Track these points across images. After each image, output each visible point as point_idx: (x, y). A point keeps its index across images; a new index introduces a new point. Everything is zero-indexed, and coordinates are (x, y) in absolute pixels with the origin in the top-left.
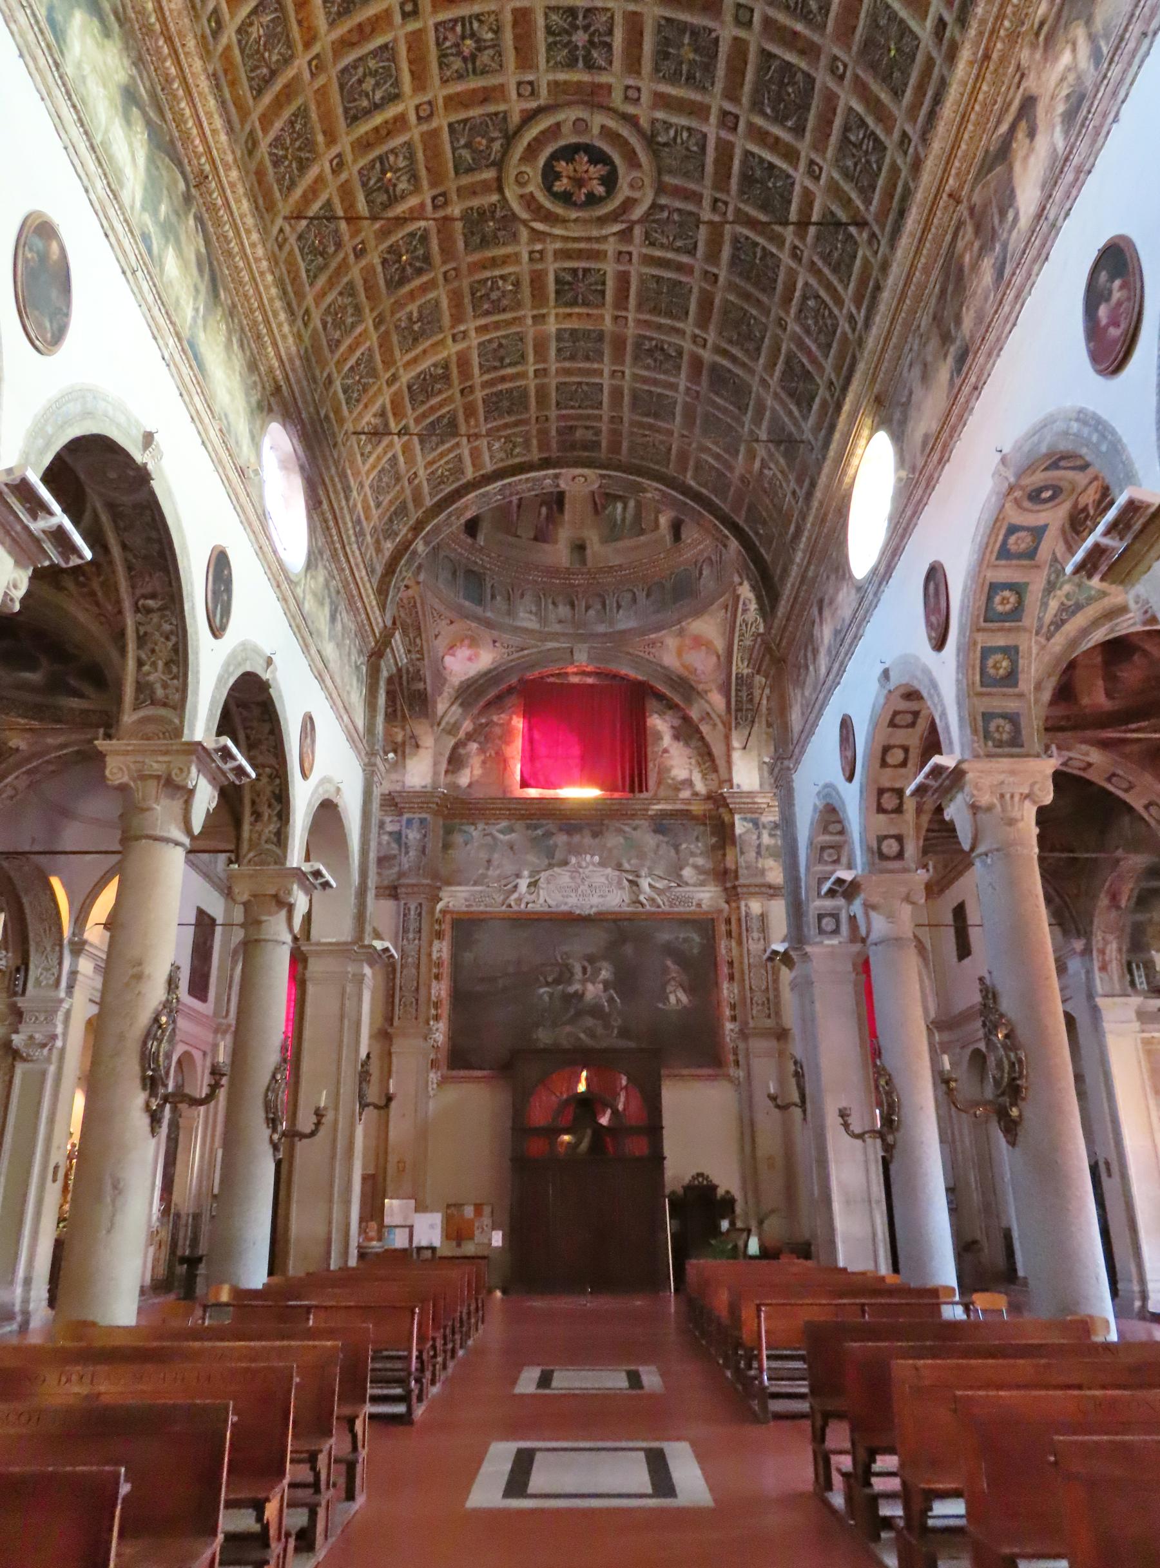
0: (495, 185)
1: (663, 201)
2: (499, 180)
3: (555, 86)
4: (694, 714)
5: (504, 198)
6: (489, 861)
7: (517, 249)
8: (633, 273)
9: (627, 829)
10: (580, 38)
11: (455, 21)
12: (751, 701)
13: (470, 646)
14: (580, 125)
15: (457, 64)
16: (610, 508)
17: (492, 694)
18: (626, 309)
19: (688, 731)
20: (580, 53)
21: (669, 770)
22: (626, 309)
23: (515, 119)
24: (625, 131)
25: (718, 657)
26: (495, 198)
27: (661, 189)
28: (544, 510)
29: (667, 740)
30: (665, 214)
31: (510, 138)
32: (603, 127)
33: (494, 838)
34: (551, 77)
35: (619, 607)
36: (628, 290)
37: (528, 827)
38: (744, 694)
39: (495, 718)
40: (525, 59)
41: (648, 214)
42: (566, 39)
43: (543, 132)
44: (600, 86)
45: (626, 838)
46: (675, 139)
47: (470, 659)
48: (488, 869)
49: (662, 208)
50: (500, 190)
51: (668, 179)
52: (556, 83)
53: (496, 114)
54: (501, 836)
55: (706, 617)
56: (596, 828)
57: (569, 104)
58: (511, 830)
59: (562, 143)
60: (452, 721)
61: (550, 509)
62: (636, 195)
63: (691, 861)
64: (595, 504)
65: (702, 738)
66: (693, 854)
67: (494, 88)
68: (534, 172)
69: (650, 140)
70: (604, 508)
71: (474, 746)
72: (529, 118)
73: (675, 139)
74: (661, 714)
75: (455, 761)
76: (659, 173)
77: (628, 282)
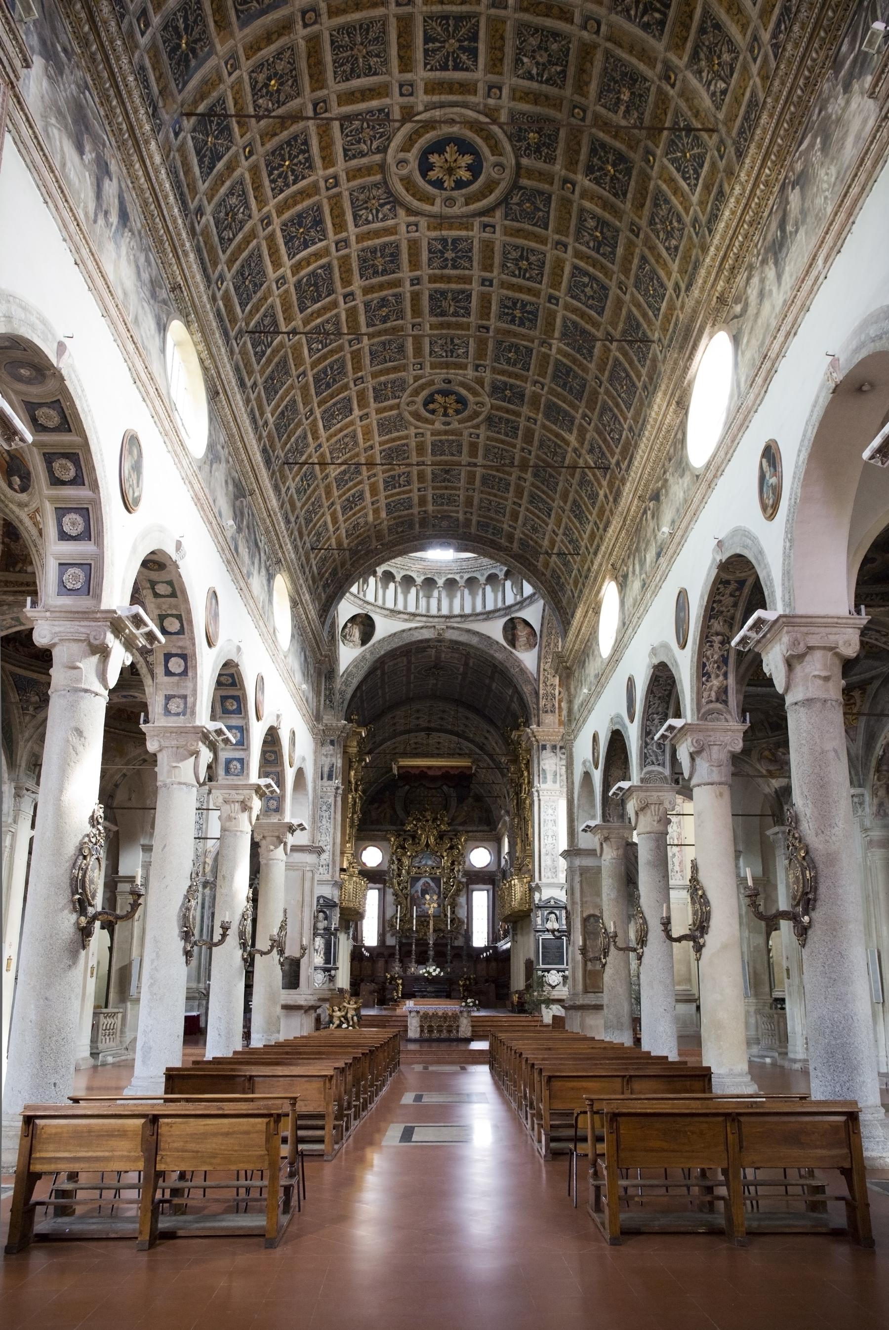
0: (523, 171)
1: (378, 157)
2: (518, 175)
3: (468, 227)
5: (517, 158)
7: (512, 104)
8: (395, 70)
10: (449, 255)
11: (528, 279)
14: (450, 201)
15: (533, 258)
18: (399, 18)
20: (450, 247)
22: (399, 18)
23: (499, 214)
24: (416, 204)
26: (525, 161)
27: (382, 167)
30: (374, 146)
31: (505, 200)
32: (433, 204)
34: (471, 233)
36: (410, 255)
40: (488, 246)
41: (389, 139)
42: (460, 254)
43: (479, 200)
44: (435, 229)
46: (378, 211)
49: (378, 151)
50: (518, 164)
51: (378, 177)
52: (467, 229)
53: (512, 220)
57: (458, 217)
59: (464, 191)
62: (402, 155)
67: (511, 235)
68: (488, 171)
69: (395, 202)
72: (488, 211)
73: (378, 211)
76: (385, 183)
77: (400, 58)
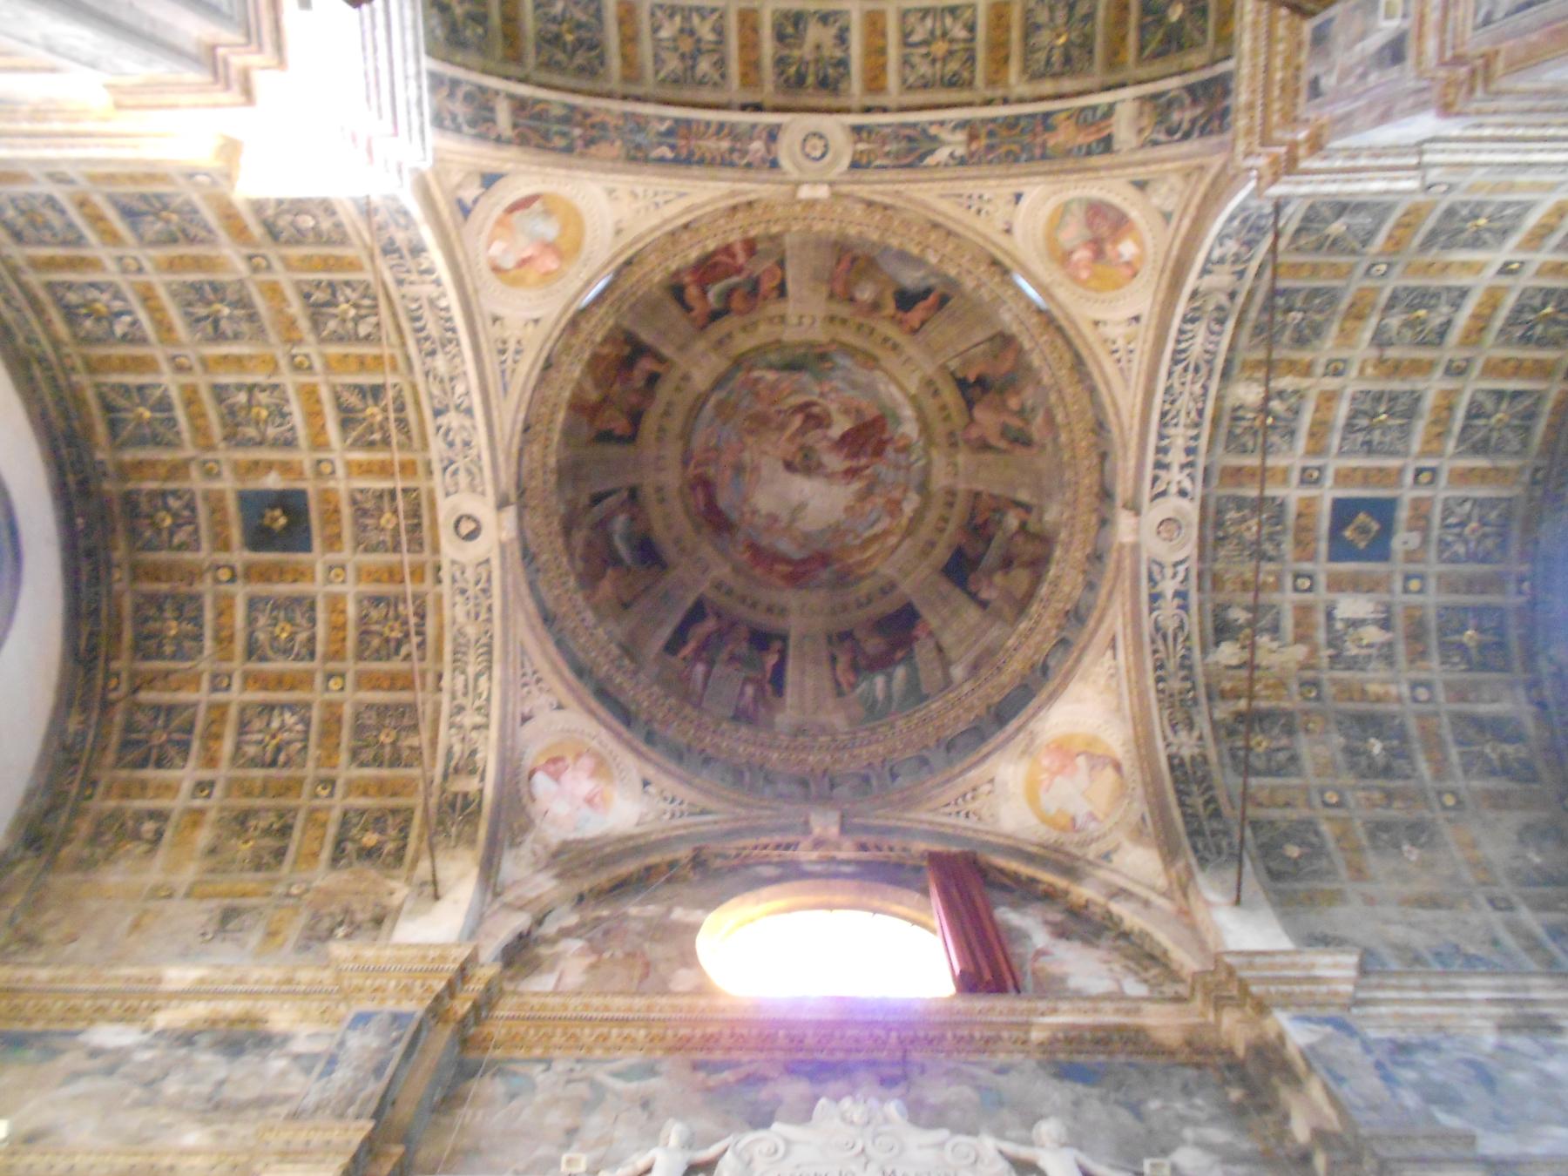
4: (1084, 892)
6: (572, 1132)
9: (981, 1072)
12: (1216, 814)
13: (594, 774)
16: (864, 686)
17: (630, 867)
19: (1081, 924)
21: (1062, 979)
25: (1118, 767)
28: (750, 690)
29: (1041, 938)
33: (594, 1085)
35: (894, 776)
37: (696, 1067)
38: (1198, 801)
39: (633, 910)
45: (978, 1088)
47: (589, 801)
48: (566, 1146)
54: (619, 1085)
55: (1075, 688)
56: (887, 1071)
58: (650, 1071)
60: (533, 895)
61: (760, 690)
63: (1189, 1133)
64: (838, 684)
65: (1125, 935)
66: (1184, 1120)
70: (853, 686)
71: (575, 945)
74: (1014, 906)
75: (521, 954)
